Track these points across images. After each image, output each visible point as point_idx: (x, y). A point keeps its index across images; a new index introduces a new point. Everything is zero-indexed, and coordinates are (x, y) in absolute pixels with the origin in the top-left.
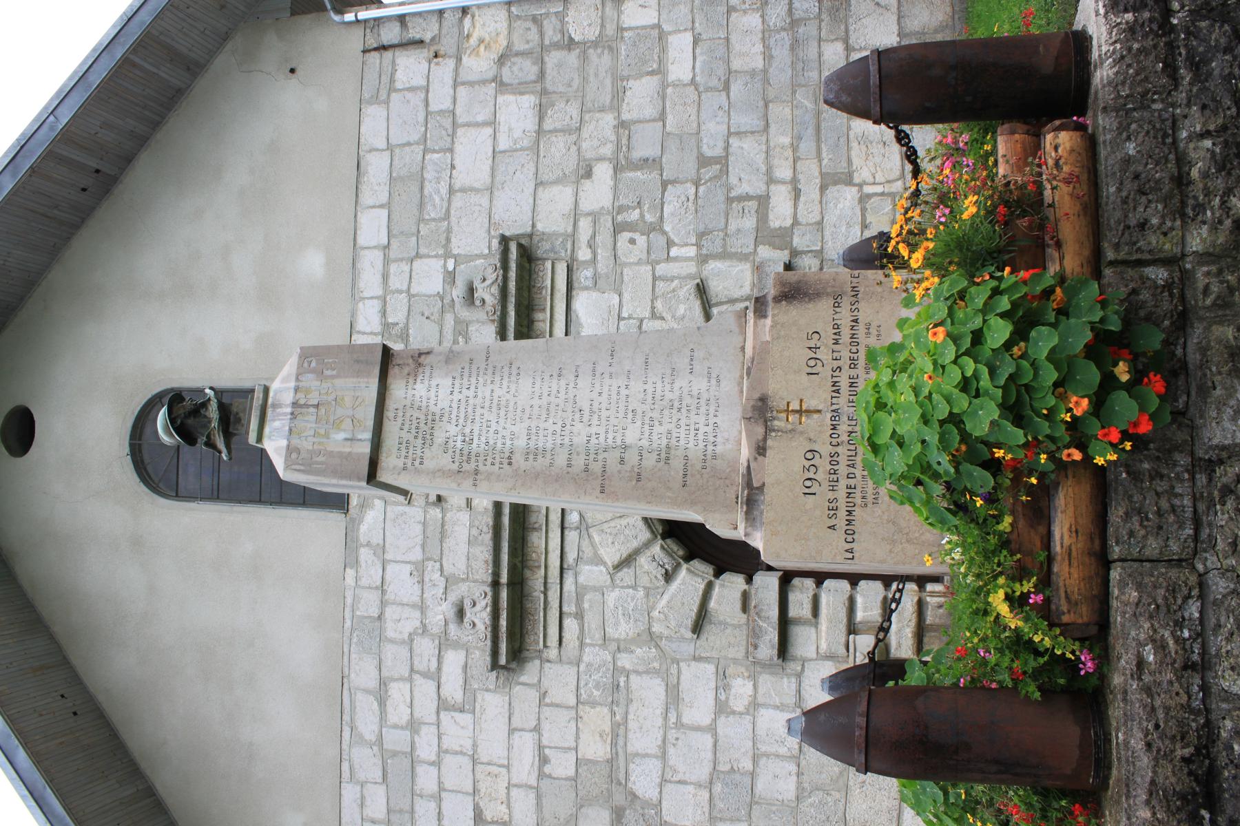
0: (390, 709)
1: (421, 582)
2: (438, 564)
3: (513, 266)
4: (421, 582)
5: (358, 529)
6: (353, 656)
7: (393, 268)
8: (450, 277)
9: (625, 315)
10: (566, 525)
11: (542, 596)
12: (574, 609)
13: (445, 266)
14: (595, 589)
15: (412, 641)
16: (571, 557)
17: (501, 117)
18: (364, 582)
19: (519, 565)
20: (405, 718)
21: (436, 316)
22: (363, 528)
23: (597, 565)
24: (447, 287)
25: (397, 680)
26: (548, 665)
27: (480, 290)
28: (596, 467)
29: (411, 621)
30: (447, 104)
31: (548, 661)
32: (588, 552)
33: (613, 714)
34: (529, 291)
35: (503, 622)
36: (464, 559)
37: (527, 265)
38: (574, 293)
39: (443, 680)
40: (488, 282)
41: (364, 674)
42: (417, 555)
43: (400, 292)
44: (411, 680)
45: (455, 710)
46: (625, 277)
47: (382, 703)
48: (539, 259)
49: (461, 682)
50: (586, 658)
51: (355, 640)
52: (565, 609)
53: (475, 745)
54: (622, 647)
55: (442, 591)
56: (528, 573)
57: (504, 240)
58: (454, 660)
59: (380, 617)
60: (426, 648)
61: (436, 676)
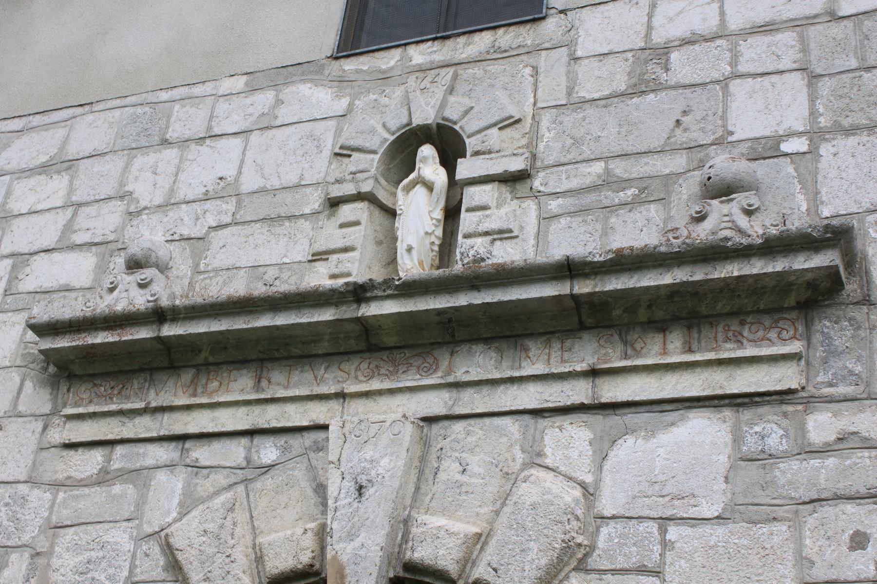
1: (207, 198)
2: (228, 219)
3: (778, 265)
4: (207, 198)
5: (304, 81)
6: (117, 113)
7: (787, 38)
8: (767, 149)
9: (673, 532)
10: (257, 440)
11: (142, 405)
12: (116, 465)
13: (791, 134)
14: (140, 504)
15: (122, 198)
16: (202, 453)
18: (223, 107)
19: (200, 359)
21: (680, 137)
22: (305, 89)
23: (181, 504)
24: (743, 148)
25: (71, 183)
26: (40, 429)
27: (725, 208)
29: (146, 191)
31: (45, 428)
32: (205, 485)
34: (731, 314)
35: (101, 338)
36: (229, 262)
37: (791, 301)
38: (727, 413)
39: (56, 256)
40: (743, 221)
41: (90, 133)
42: (250, 182)
43: (734, 63)
45: (9, 282)
46: (765, 529)
47: (45, 169)
48: (808, 325)
49: (47, 285)
50: (36, 492)
51: (139, 110)
52: (119, 450)
54: (41, 561)
55: (186, 233)
56: (187, 376)
57: (838, 236)
58: (77, 269)
59: (165, 142)
60: (103, 222)
61: (65, 245)
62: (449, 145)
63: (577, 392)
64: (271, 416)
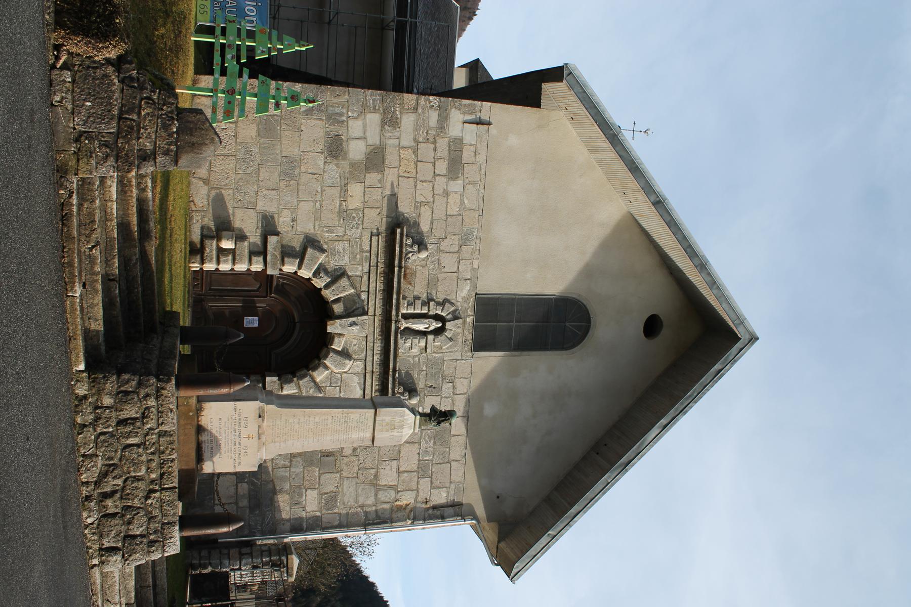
0: (458, 201)
16: (365, 278)
17: (396, 475)
20: (450, 198)
22: (468, 288)
28: (307, 417)
30: (422, 481)
33: (346, 206)
44: (448, 216)
52: (368, 254)
53: (416, 186)
62: (438, 332)
63: (369, 369)
64: (372, 297)
